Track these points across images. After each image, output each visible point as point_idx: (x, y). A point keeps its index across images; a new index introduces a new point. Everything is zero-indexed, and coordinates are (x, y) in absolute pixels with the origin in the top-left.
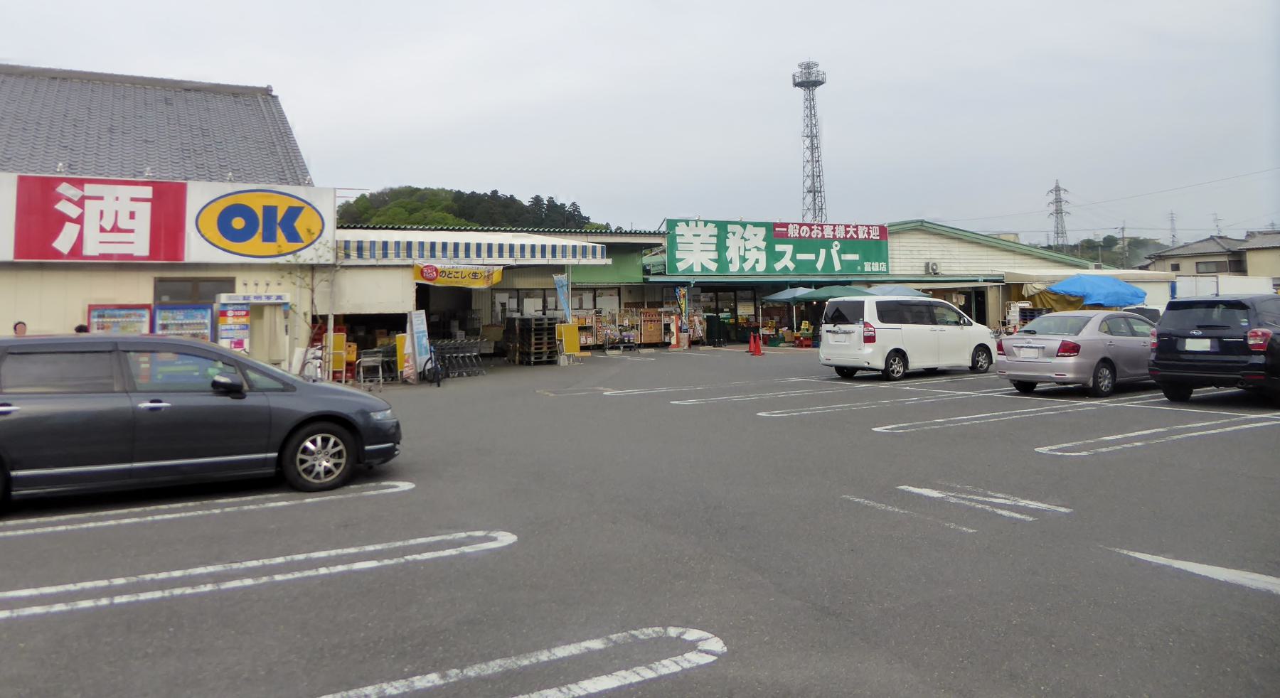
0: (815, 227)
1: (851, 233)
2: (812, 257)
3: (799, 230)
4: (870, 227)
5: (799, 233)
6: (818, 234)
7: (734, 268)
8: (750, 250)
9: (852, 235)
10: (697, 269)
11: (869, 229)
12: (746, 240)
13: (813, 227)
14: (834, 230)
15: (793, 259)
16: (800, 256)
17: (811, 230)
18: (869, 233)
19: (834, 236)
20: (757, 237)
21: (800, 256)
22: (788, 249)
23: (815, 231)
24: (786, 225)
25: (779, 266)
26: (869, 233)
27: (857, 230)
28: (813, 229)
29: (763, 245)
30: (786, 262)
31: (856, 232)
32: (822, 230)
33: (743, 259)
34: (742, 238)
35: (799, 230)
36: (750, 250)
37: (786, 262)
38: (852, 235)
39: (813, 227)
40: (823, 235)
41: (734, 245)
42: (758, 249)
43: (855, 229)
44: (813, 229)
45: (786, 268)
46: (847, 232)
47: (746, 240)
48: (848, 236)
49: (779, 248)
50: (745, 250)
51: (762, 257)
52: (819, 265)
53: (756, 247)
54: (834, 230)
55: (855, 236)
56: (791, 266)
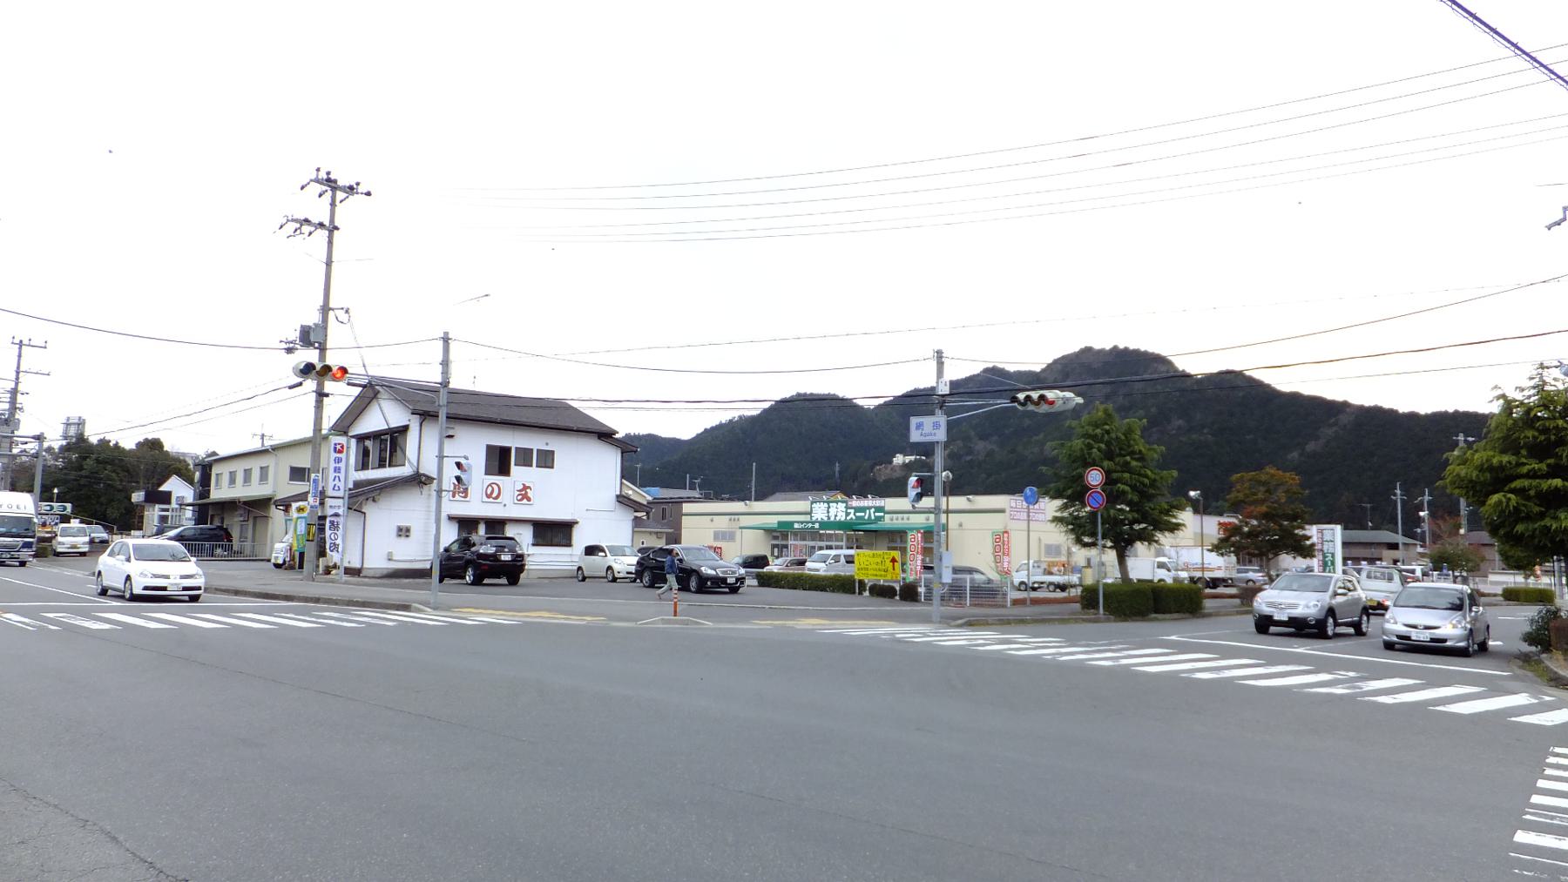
7: (832, 519)
16: (858, 514)
21: (858, 514)
22: (852, 511)
25: (848, 518)
29: (844, 510)
30: (852, 516)
37: (852, 516)
45: (852, 519)
49: (849, 511)
52: (866, 517)
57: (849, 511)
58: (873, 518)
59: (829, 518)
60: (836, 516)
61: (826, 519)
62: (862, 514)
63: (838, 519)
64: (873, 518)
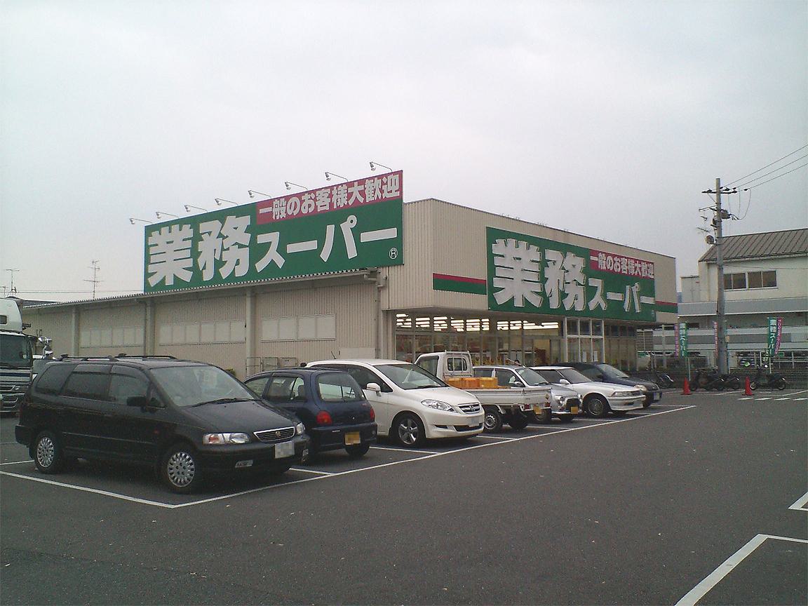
0: (305, 197)
1: (356, 194)
2: (312, 245)
4: (385, 180)
6: (310, 206)
7: (208, 275)
8: (228, 249)
10: (169, 282)
11: (383, 183)
12: (224, 238)
14: (331, 196)
15: (281, 250)
16: (292, 248)
17: (302, 202)
18: (382, 191)
19: (331, 204)
20: (238, 229)
21: (292, 248)
22: (273, 238)
24: (269, 203)
26: (382, 191)
29: (246, 239)
30: (273, 255)
31: (362, 193)
32: (315, 200)
33: (219, 264)
34: (220, 235)
36: (228, 249)
37: (273, 255)
39: (303, 198)
41: (208, 248)
42: (241, 246)
43: (361, 188)
44: (304, 200)
46: (350, 195)
47: (224, 238)
49: (262, 239)
50: (223, 249)
51: (244, 254)
52: (325, 256)
53: (236, 243)
54: (331, 196)
55: (361, 200)
56: (280, 262)
57: (262, 239)
58: (352, 253)
59: (195, 269)
60: (219, 264)
61: (187, 276)
62: (312, 245)
63: (225, 272)
64: (352, 253)
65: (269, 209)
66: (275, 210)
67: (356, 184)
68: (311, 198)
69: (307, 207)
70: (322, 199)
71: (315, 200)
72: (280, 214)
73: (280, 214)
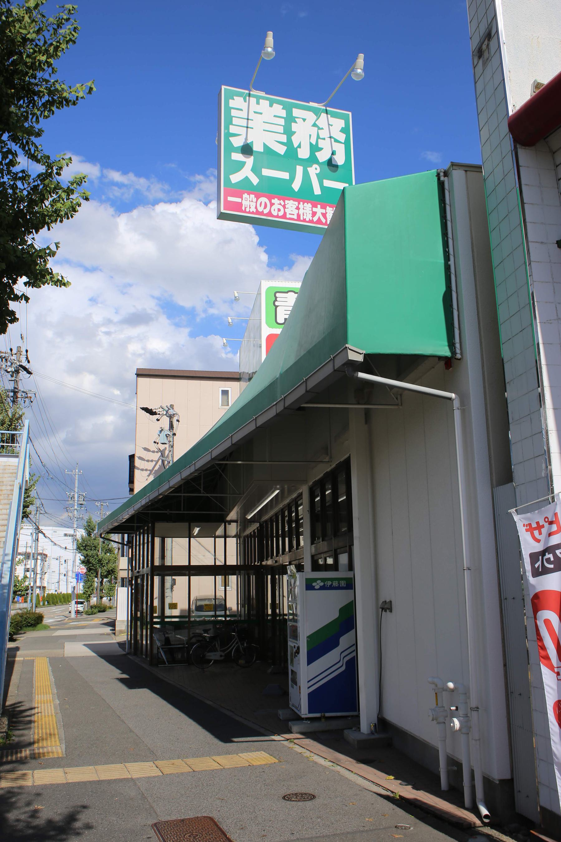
3: (256, 202)
5: (256, 208)
6: (279, 210)
9: (319, 217)
13: (273, 201)
17: (272, 204)
23: (276, 207)
27: (326, 213)
28: (274, 204)
32: (284, 207)
35: (256, 202)
38: (319, 217)
39: (273, 201)
40: (285, 213)
43: (324, 211)
44: (274, 204)
46: (314, 214)
48: (315, 219)
65: (238, 200)
66: (244, 203)
67: (319, 206)
68: (280, 204)
69: (276, 210)
70: (292, 209)
71: (284, 207)
72: (250, 208)
73: (250, 208)
